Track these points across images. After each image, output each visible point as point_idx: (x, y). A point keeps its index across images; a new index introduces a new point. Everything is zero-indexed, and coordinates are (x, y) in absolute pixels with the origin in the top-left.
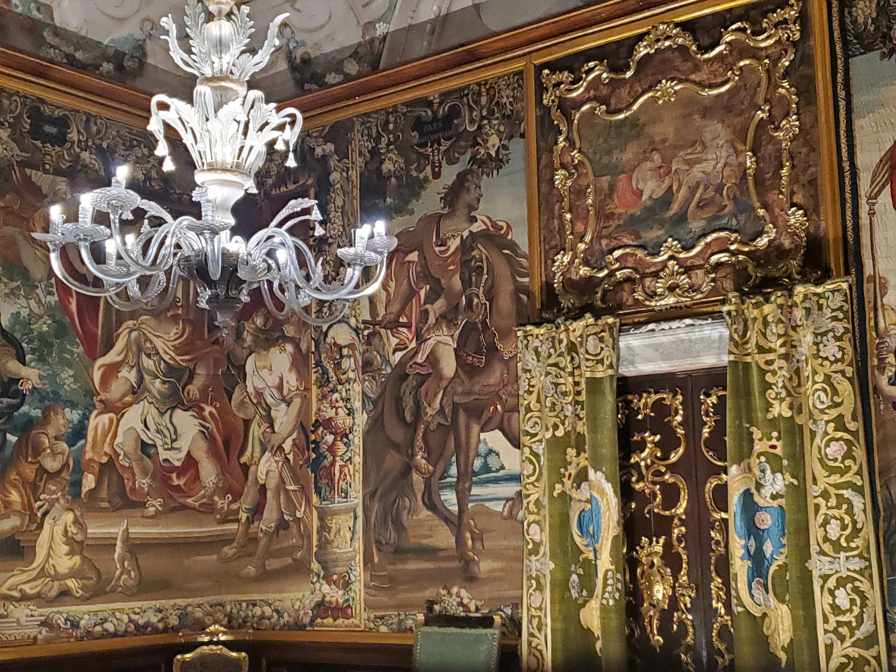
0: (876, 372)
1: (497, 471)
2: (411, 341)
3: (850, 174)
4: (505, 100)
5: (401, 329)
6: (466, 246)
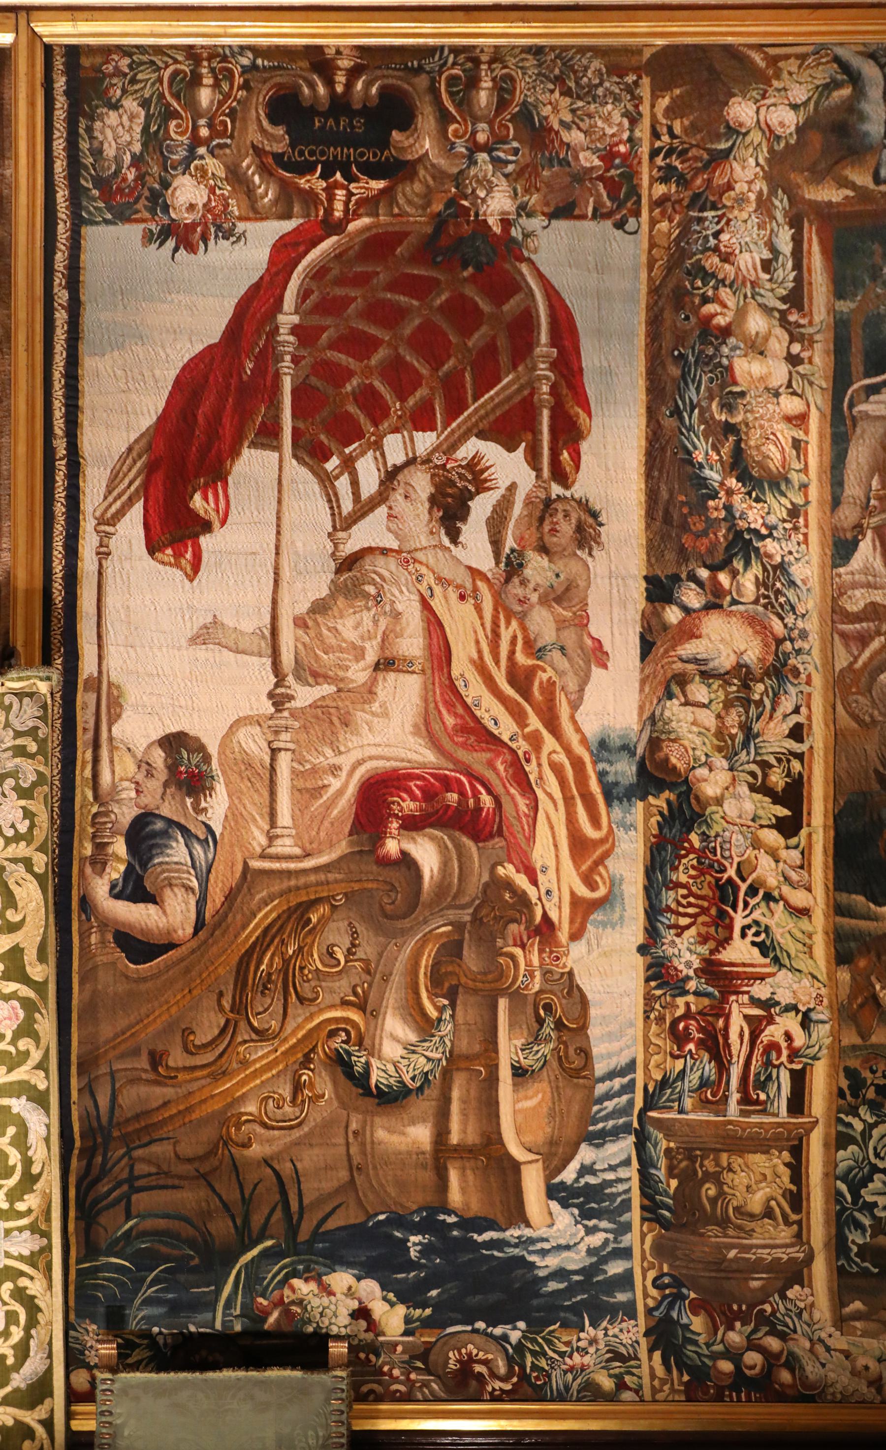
0: (88, 870)
3: (68, 466)
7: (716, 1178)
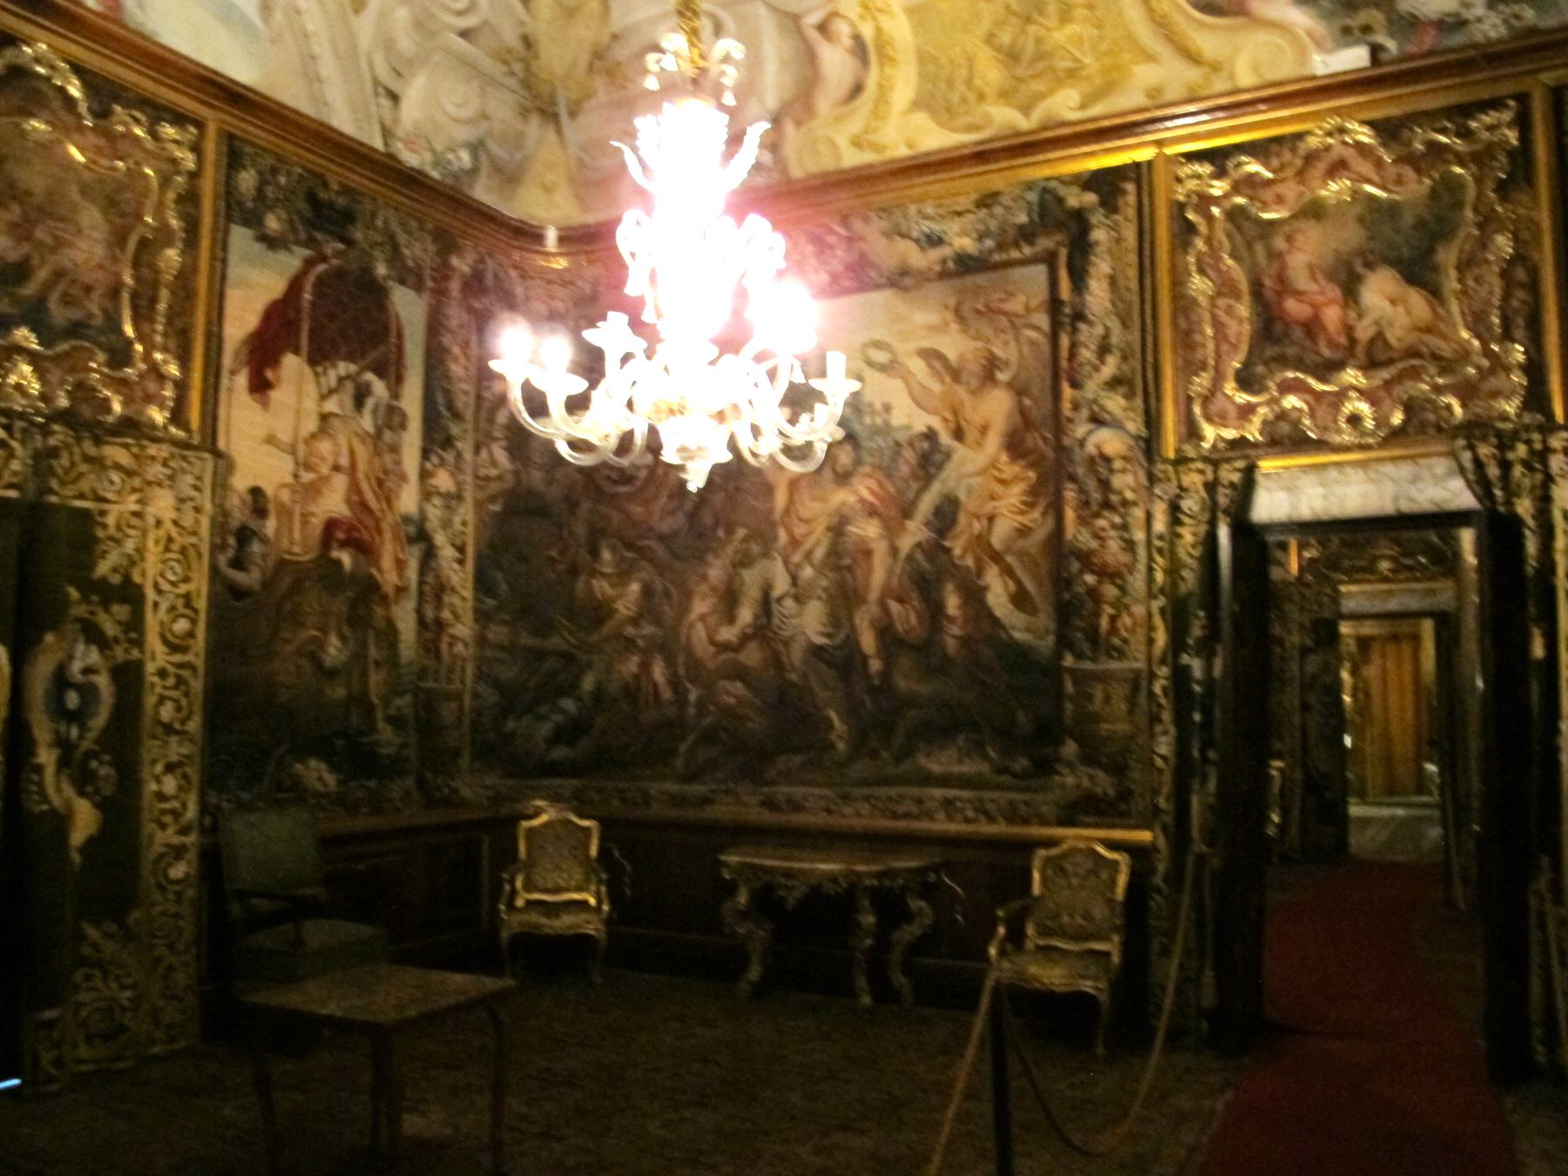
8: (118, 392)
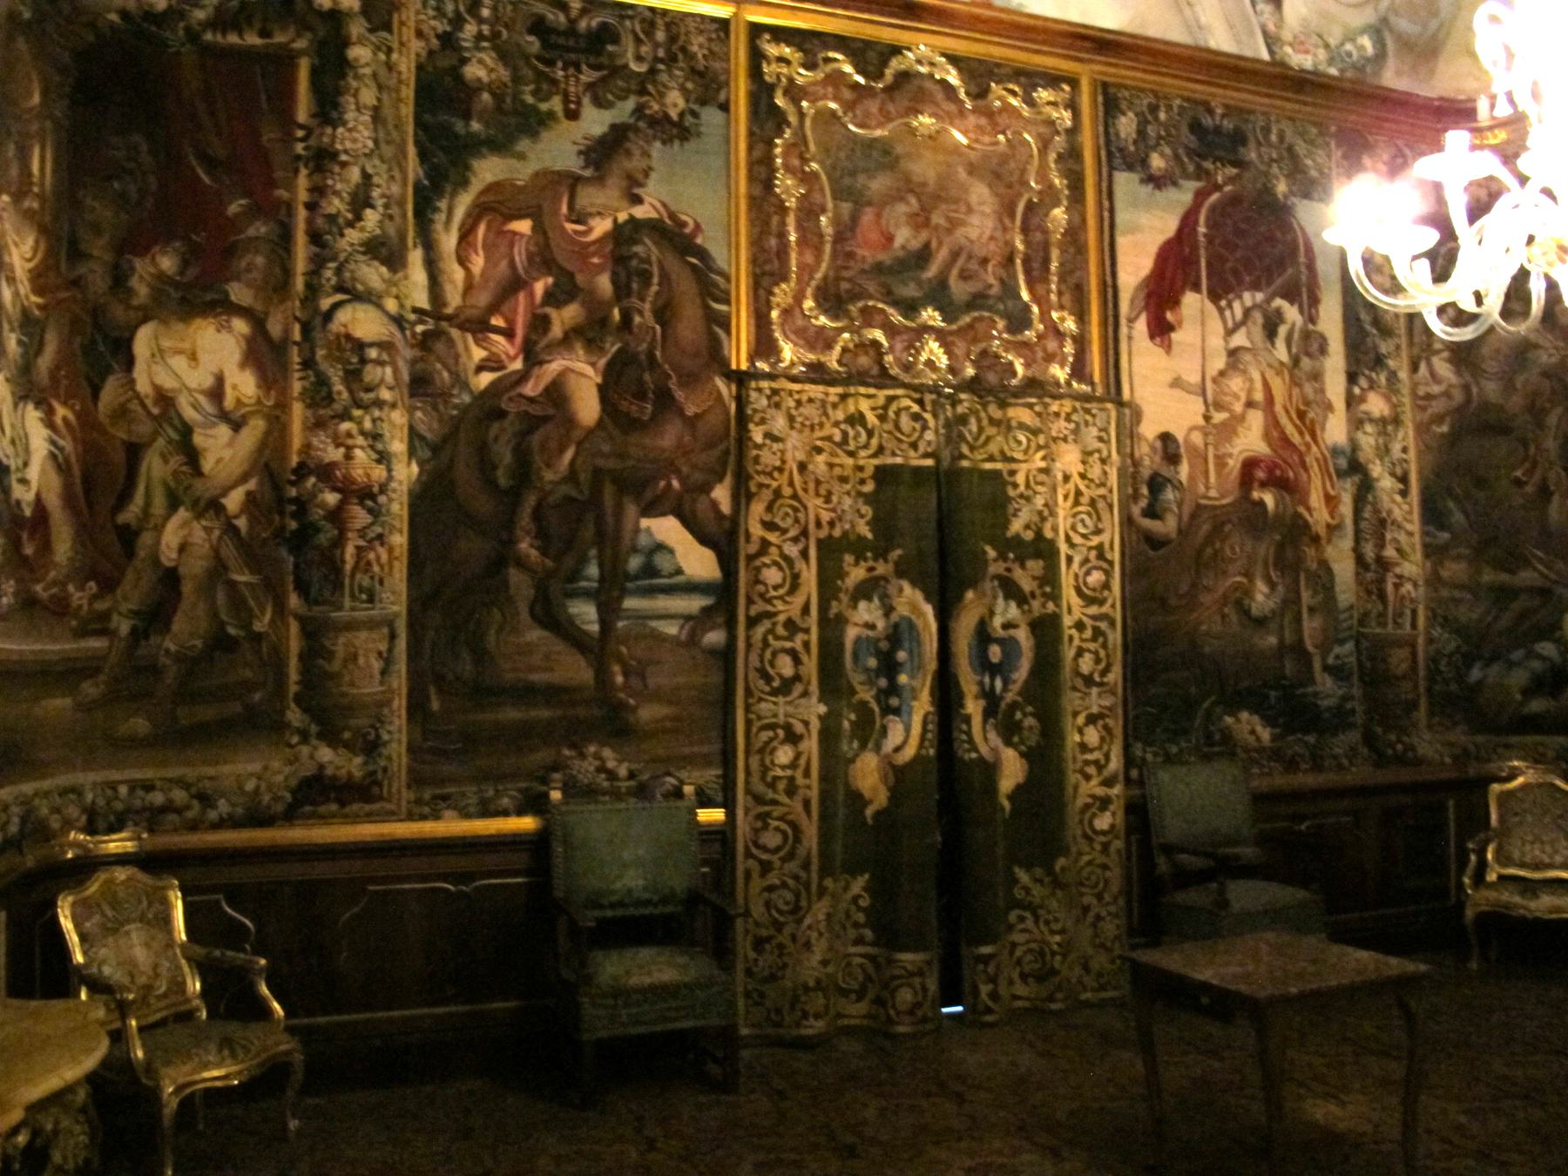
1: (671, 575)
2: (513, 359)
4: (695, 48)
5: (494, 337)
6: (625, 234)
7: (1384, 660)
8: (1020, 356)
